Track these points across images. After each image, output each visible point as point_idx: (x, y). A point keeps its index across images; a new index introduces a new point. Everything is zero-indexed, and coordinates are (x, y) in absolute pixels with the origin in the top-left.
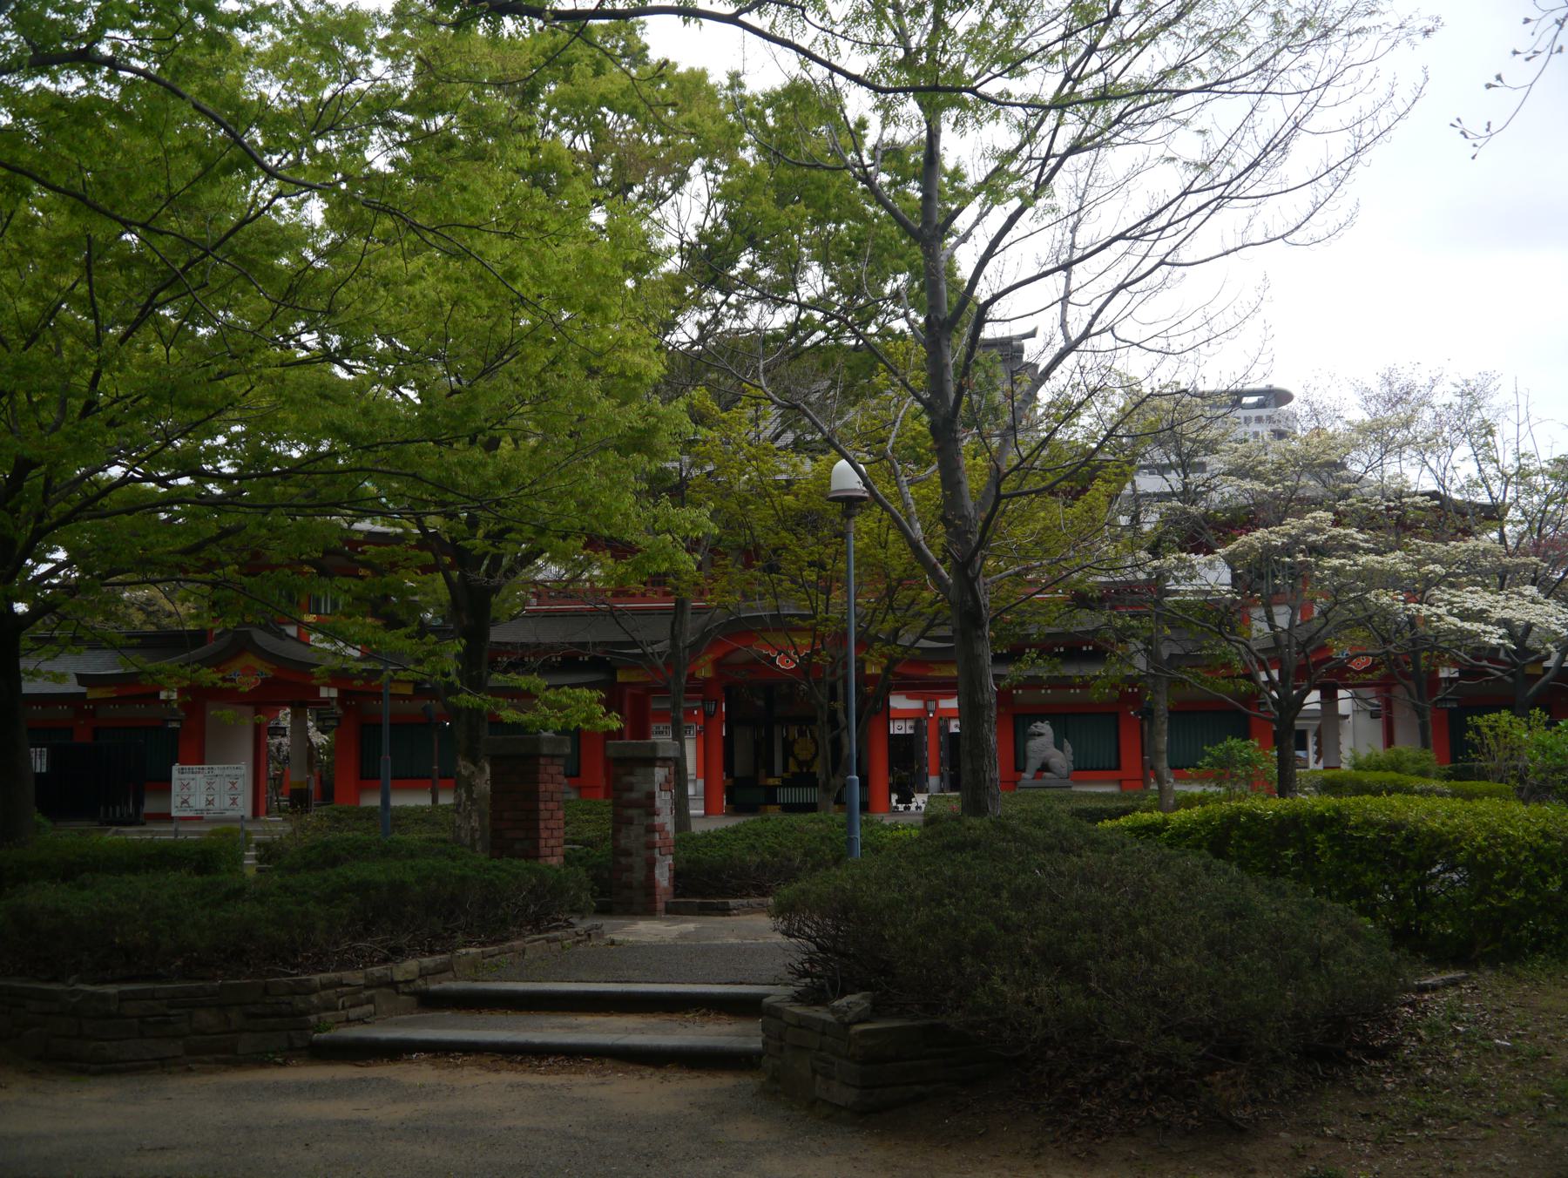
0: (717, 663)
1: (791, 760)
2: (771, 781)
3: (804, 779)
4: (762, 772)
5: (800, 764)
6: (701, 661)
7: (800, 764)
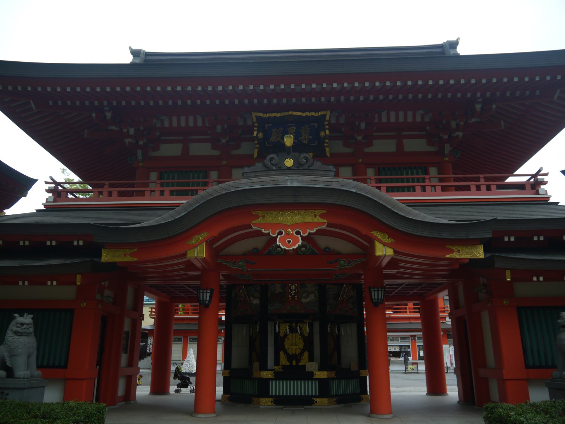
0: (210, 243)
1: (282, 354)
2: (265, 374)
3: (295, 372)
4: (256, 365)
5: (290, 357)
7: (290, 357)
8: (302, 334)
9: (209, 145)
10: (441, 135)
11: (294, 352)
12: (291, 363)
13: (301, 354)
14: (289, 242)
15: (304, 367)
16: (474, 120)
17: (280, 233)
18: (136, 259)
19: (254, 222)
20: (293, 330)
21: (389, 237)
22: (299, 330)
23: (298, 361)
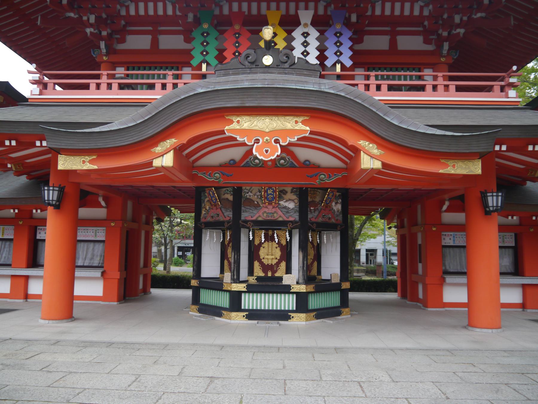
0: (178, 151)
1: (256, 264)
3: (271, 285)
5: (265, 268)
6: (158, 149)
7: (265, 268)
8: (279, 243)
9: (182, 37)
10: (440, 31)
11: (270, 262)
12: (266, 273)
13: (278, 264)
14: (267, 151)
15: (281, 279)
16: (479, 15)
17: (257, 141)
18: (95, 167)
19: (227, 128)
20: (269, 238)
21: (378, 148)
22: (276, 237)
23: (274, 272)
